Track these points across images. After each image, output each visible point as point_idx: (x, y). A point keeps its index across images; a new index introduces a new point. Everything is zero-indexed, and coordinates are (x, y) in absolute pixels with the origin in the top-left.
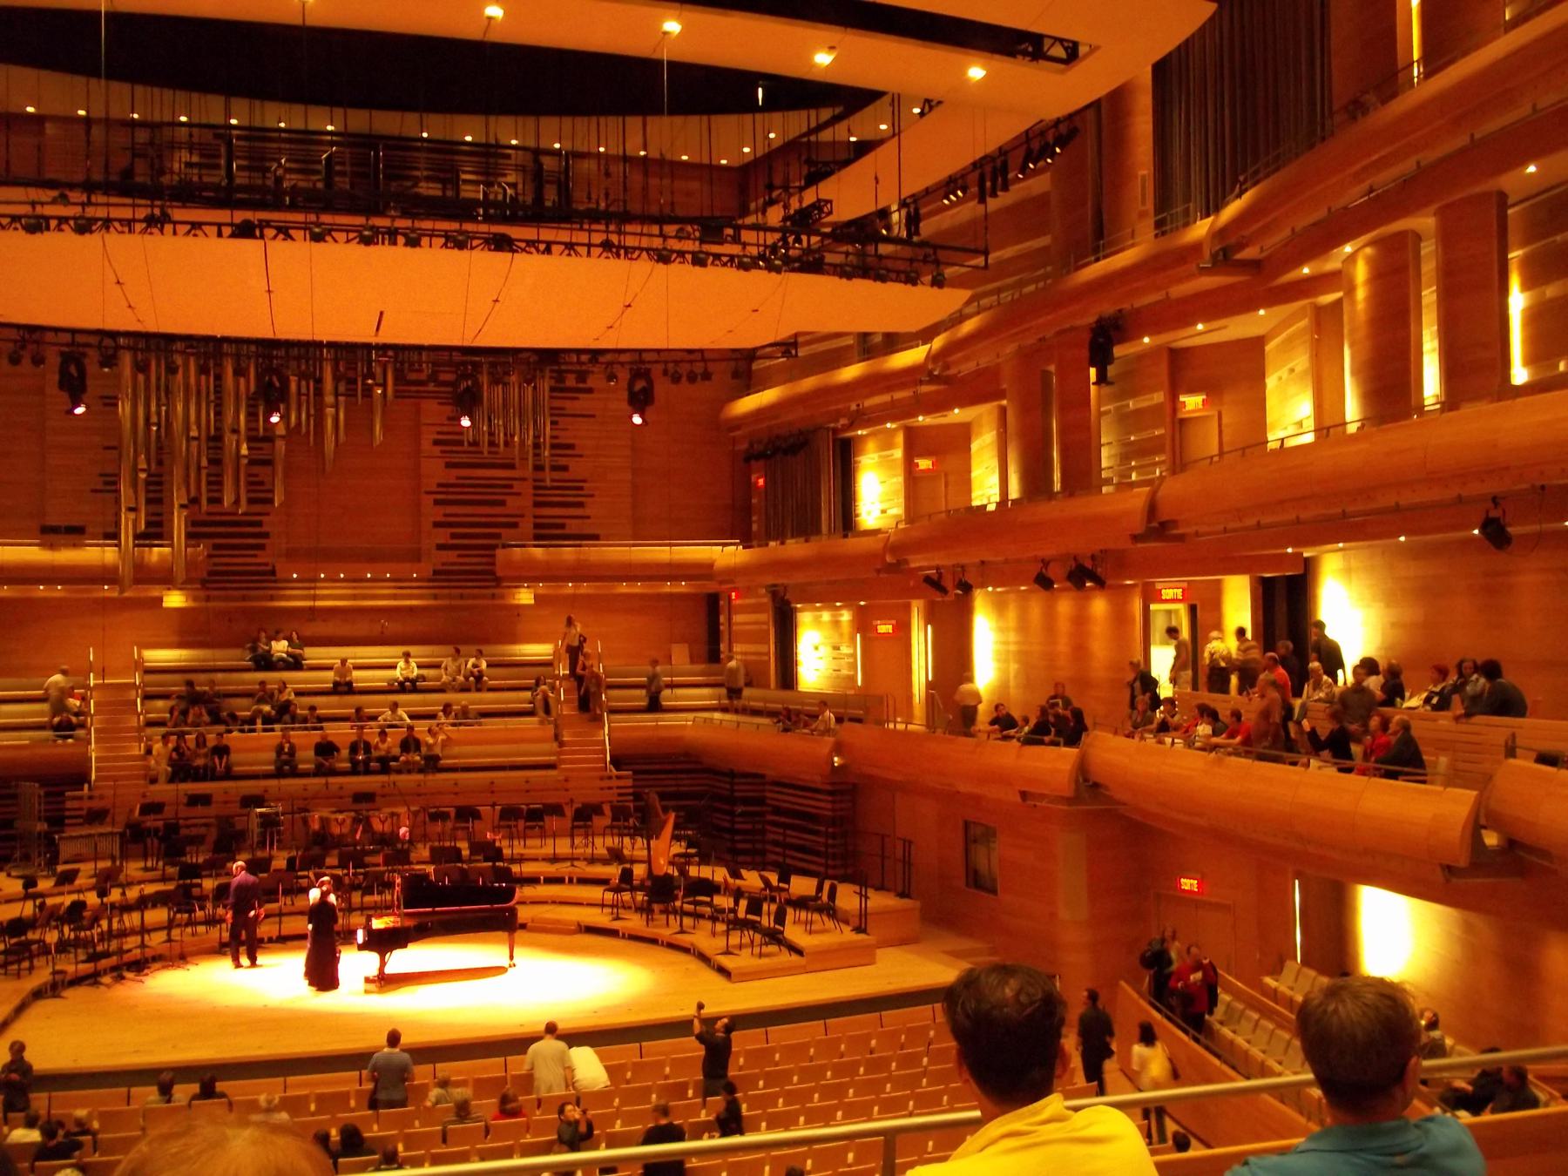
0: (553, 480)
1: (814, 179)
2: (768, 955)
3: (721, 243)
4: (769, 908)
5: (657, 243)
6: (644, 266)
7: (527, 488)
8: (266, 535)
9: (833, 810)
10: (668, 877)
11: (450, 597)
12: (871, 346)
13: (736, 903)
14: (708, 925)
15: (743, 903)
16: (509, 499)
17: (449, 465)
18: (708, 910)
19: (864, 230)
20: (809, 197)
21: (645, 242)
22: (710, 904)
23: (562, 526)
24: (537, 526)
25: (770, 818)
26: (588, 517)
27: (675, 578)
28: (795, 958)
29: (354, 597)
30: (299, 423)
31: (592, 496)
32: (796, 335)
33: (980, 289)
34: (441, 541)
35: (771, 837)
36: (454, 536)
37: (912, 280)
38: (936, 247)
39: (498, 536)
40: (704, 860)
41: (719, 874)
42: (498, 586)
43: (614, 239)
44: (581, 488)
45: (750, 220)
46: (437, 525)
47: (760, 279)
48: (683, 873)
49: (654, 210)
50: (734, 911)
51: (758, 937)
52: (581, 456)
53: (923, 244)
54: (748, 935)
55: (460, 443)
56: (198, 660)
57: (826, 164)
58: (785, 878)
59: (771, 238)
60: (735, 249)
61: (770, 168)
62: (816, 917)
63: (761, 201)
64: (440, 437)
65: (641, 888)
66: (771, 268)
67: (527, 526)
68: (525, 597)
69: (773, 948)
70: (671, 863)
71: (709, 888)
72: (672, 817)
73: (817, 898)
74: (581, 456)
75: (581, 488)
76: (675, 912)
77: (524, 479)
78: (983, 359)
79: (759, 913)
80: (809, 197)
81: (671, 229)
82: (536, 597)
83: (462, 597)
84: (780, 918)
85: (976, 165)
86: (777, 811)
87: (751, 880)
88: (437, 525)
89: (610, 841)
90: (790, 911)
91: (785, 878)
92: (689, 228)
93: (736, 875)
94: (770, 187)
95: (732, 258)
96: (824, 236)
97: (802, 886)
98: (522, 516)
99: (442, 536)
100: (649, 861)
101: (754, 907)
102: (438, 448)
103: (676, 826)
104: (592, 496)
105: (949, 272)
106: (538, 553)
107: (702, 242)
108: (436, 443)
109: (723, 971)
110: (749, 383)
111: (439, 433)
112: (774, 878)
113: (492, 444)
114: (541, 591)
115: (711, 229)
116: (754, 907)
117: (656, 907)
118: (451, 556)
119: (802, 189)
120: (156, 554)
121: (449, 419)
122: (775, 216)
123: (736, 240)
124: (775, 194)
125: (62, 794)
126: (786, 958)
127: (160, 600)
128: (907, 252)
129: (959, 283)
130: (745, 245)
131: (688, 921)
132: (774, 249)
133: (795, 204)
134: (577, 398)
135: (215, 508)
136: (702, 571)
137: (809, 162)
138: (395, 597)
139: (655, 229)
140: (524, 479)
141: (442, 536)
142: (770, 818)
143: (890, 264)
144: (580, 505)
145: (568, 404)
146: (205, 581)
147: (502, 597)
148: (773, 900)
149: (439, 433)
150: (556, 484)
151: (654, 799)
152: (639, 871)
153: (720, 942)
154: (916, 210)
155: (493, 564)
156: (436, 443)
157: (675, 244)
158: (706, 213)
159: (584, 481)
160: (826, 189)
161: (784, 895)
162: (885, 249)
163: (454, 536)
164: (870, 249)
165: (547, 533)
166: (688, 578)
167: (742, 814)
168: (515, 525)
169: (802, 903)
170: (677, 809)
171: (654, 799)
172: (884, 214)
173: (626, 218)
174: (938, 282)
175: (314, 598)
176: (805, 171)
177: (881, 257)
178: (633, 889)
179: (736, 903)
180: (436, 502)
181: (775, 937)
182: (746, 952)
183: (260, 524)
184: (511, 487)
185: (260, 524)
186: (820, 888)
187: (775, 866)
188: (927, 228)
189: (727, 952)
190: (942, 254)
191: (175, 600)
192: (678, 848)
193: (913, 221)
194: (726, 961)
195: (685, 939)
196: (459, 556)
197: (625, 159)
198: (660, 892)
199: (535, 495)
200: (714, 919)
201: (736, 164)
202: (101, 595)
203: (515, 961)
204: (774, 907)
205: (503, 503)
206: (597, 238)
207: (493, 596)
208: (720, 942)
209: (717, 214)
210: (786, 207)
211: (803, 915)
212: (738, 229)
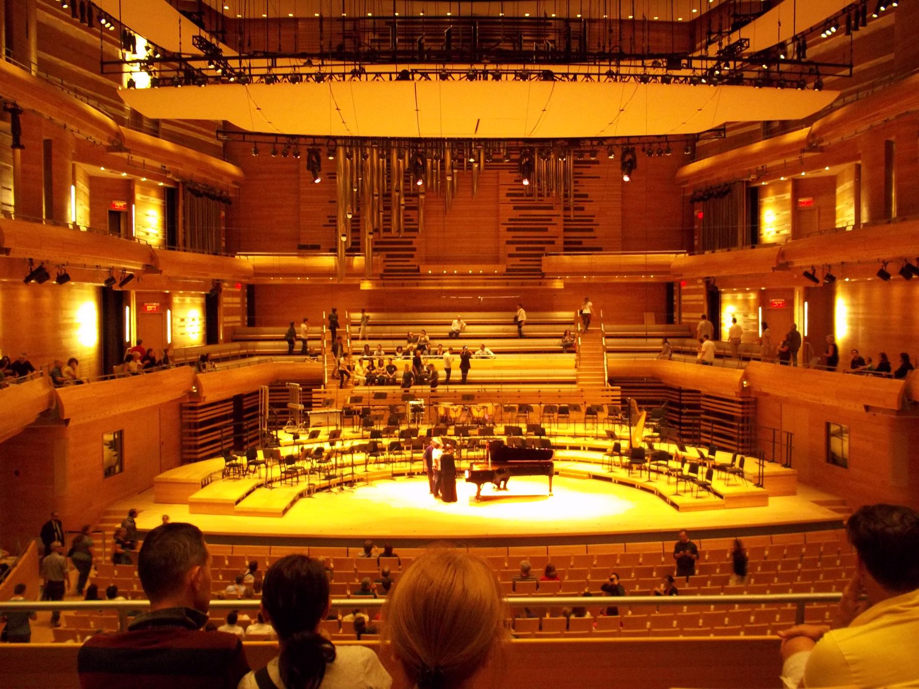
0: (575, 216)
1: (737, 27)
2: (700, 497)
3: (680, 69)
4: (703, 470)
5: (640, 71)
6: (632, 85)
7: (559, 221)
8: (414, 249)
9: (742, 413)
10: (641, 450)
11: (516, 284)
12: (771, 129)
13: (683, 466)
14: (665, 477)
15: (687, 467)
16: (550, 227)
17: (515, 208)
18: (665, 469)
19: (769, 55)
20: (735, 38)
21: (632, 71)
22: (666, 466)
23: (580, 243)
24: (565, 243)
25: (703, 416)
26: (595, 238)
27: (647, 273)
28: (718, 499)
29: (463, 284)
30: (432, 186)
32: (725, 124)
33: (845, 91)
35: (702, 428)
36: (518, 249)
37: (802, 85)
38: (817, 65)
39: (543, 249)
40: (663, 439)
41: (672, 448)
42: (543, 278)
43: (614, 69)
44: (592, 221)
45: (696, 54)
46: (508, 243)
47: (705, 91)
48: (651, 447)
49: (638, 51)
50: (681, 470)
51: (695, 486)
52: (592, 201)
53: (810, 63)
54: (689, 485)
55: (522, 195)
57: (746, 16)
58: (712, 452)
59: (710, 64)
60: (688, 72)
61: (710, 21)
62: (731, 476)
63: (704, 41)
64: (509, 192)
65: (626, 454)
66: (709, 83)
67: (560, 242)
68: (559, 284)
69: (704, 493)
70: (644, 441)
71: (666, 456)
72: (645, 413)
73: (732, 465)
74: (592, 201)
76: (646, 469)
77: (559, 216)
78: (847, 133)
79: (696, 472)
80: (735, 38)
81: (649, 62)
82: (567, 286)
83: (522, 284)
84: (709, 476)
85: (844, 10)
86: (708, 413)
87: (692, 452)
88: (508, 243)
89: (609, 427)
90: (715, 472)
91: (712, 452)
92: (660, 61)
93: (682, 449)
94: (710, 33)
95: (686, 77)
96: (745, 61)
97: (722, 457)
99: (512, 249)
100: (630, 440)
101: (694, 469)
102: (509, 198)
103: (647, 420)
105: (825, 80)
106: (567, 259)
107: (668, 68)
109: (673, 505)
110: (833, 82)
111: (509, 189)
112: (705, 452)
114: (569, 281)
115: (674, 63)
116: (694, 469)
117: (634, 466)
118: (516, 261)
119: (729, 33)
120: (358, 261)
121: (516, 181)
122: (713, 50)
123: (689, 66)
124: (712, 37)
125: (310, 390)
126: (712, 498)
127: (359, 286)
128: (798, 68)
129: (832, 87)
130: (694, 69)
131: (653, 475)
132: (712, 70)
133: (725, 43)
134: (590, 167)
136: (664, 269)
137: (735, 16)
138: (485, 284)
139: (639, 63)
140: (559, 216)
141: (512, 249)
142: (703, 416)
143: (786, 77)
144: (591, 230)
145: (583, 170)
147: (545, 284)
148: (705, 465)
149: (509, 189)
151: (634, 402)
152: (624, 445)
153: (673, 489)
154: (804, 42)
155: (540, 265)
156: (508, 195)
157: (651, 71)
158: (670, 52)
159: (594, 216)
160: (745, 32)
161: (712, 463)
162: (784, 67)
163: (518, 249)
164: (774, 68)
165: (572, 247)
167: (687, 414)
168: (553, 243)
169: (722, 468)
170: (647, 409)
171: (634, 402)
172: (782, 46)
173: (619, 57)
174: (819, 86)
176: (732, 20)
177: (781, 73)
178: (621, 455)
179: (683, 466)
180: (509, 230)
181: (705, 486)
182: (689, 495)
183: (411, 243)
184: (551, 220)
185: (411, 243)
186: (734, 459)
187: (707, 445)
188: (811, 53)
189: (677, 494)
190: (821, 69)
191: (366, 286)
192: (648, 432)
193: (801, 49)
194: (676, 500)
195: (651, 485)
196: (521, 261)
197: (621, 22)
198: (637, 456)
199: (565, 225)
200: (668, 474)
201: (688, 20)
203: (552, 492)
204: (705, 469)
205: (546, 230)
206: (604, 70)
207: (540, 284)
208: (673, 489)
209: (676, 51)
210: (720, 44)
211: (723, 475)
212: (690, 60)
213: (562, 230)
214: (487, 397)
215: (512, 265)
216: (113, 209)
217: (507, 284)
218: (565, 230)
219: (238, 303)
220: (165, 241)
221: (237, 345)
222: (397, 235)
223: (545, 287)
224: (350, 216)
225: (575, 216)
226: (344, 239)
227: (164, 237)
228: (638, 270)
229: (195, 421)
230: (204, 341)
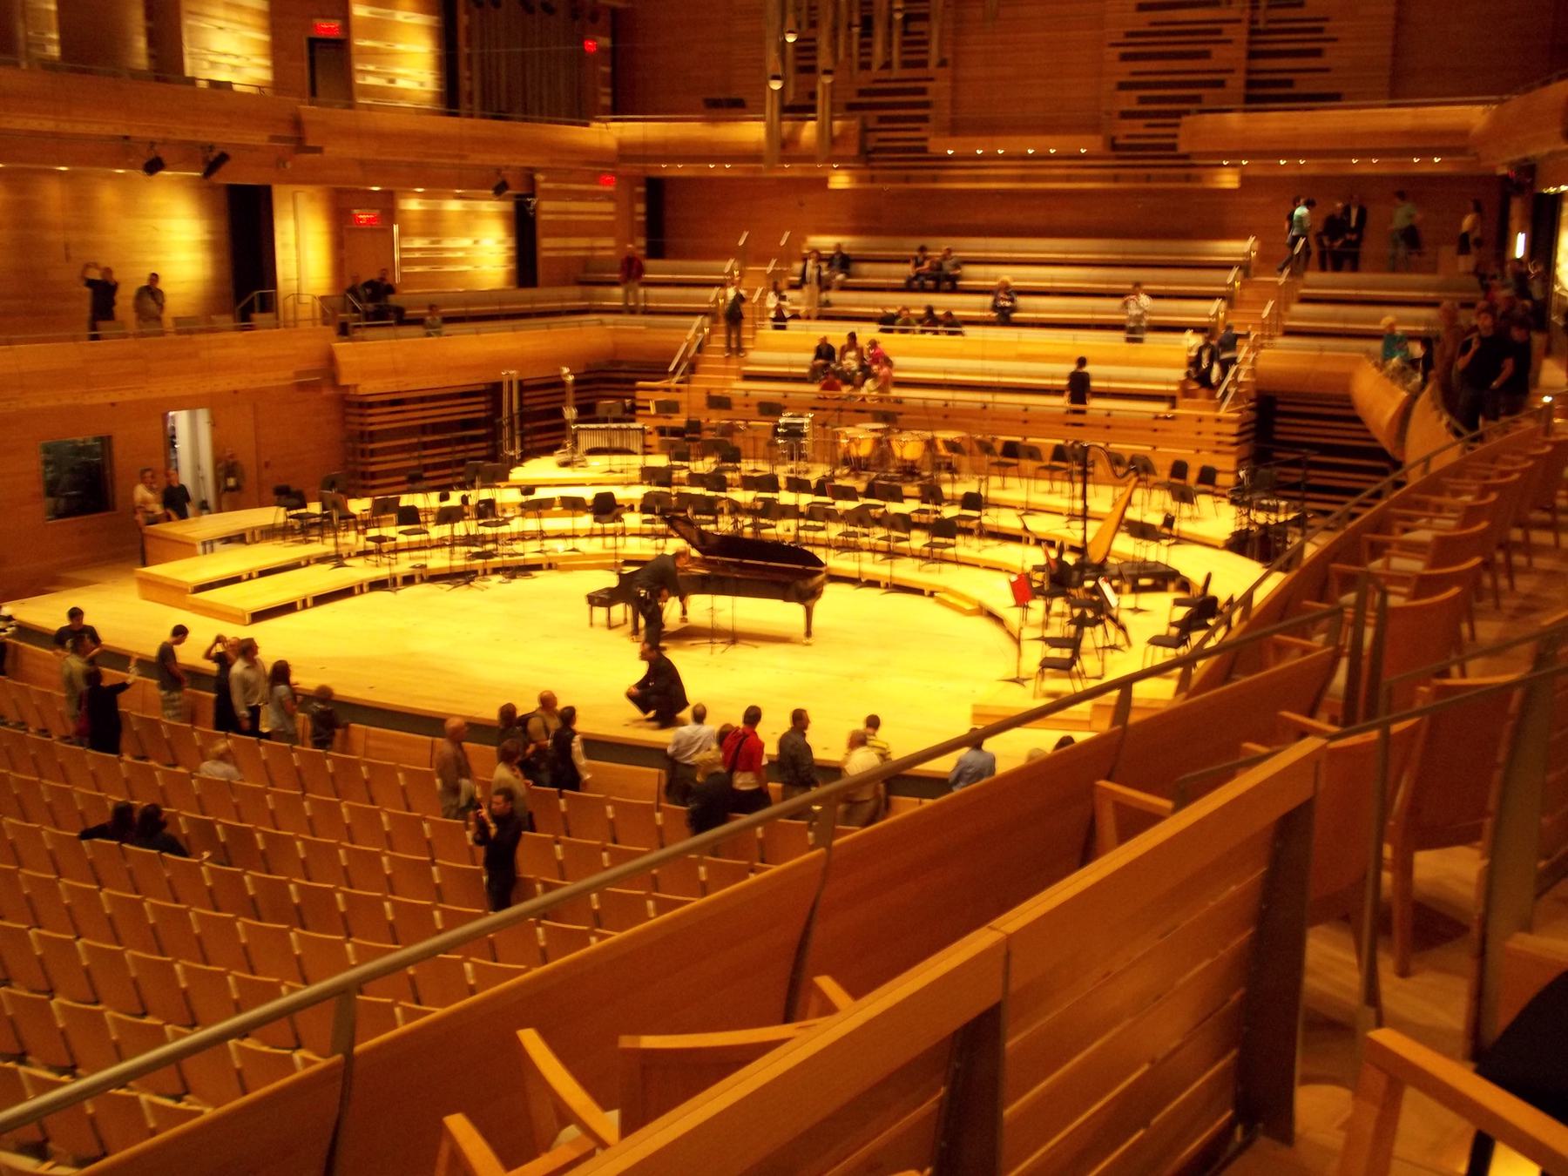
0: (1270, 21)
7: (1239, 34)
8: (926, 105)
11: (1137, 179)
23: (1289, 83)
24: (1250, 84)
26: (1326, 70)
27: (1427, 153)
29: (1022, 179)
31: (1335, 40)
34: (1126, 108)
36: (1143, 100)
39: (1196, 99)
44: (1320, 30)
46: (1123, 86)
56: (859, 249)
67: (1236, 82)
68: (1228, 180)
75: (1320, 30)
77: (1238, 21)
82: (1245, 180)
83: (1148, 178)
88: (1123, 86)
98: (1231, 71)
99: (1129, 100)
104: (1335, 40)
106: (1234, 120)
114: (1253, 172)
118: (1138, 126)
127: (825, 181)
135: (885, 74)
136: (1453, 142)
138: (1068, 179)
140: (1238, 21)
141: (1129, 100)
144: (1317, 53)
146: (866, 157)
147: (1199, 179)
150: (1272, 26)
159: (1326, 19)
163: (1143, 100)
165: (1260, 95)
166: (1307, 154)
168: (1220, 84)
175: (978, 179)
180: (1125, 57)
183: (923, 91)
184: (1219, 32)
185: (923, 91)
191: (840, 180)
196: (1149, 126)
202: (780, 174)
205: (1206, 55)
207: (1188, 178)
213: (1243, 54)
214: (947, 417)
215: (1128, 137)
216: (314, 35)
217: (1116, 179)
218: (1252, 55)
219: (610, 213)
220: (440, 94)
221: (576, 291)
222: (885, 74)
223: (1198, 186)
224: (791, 39)
225: (1270, 21)
226: (776, 85)
227: (441, 87)
228: (1387, 144)
229: (363, 428)
230: (509, 283)
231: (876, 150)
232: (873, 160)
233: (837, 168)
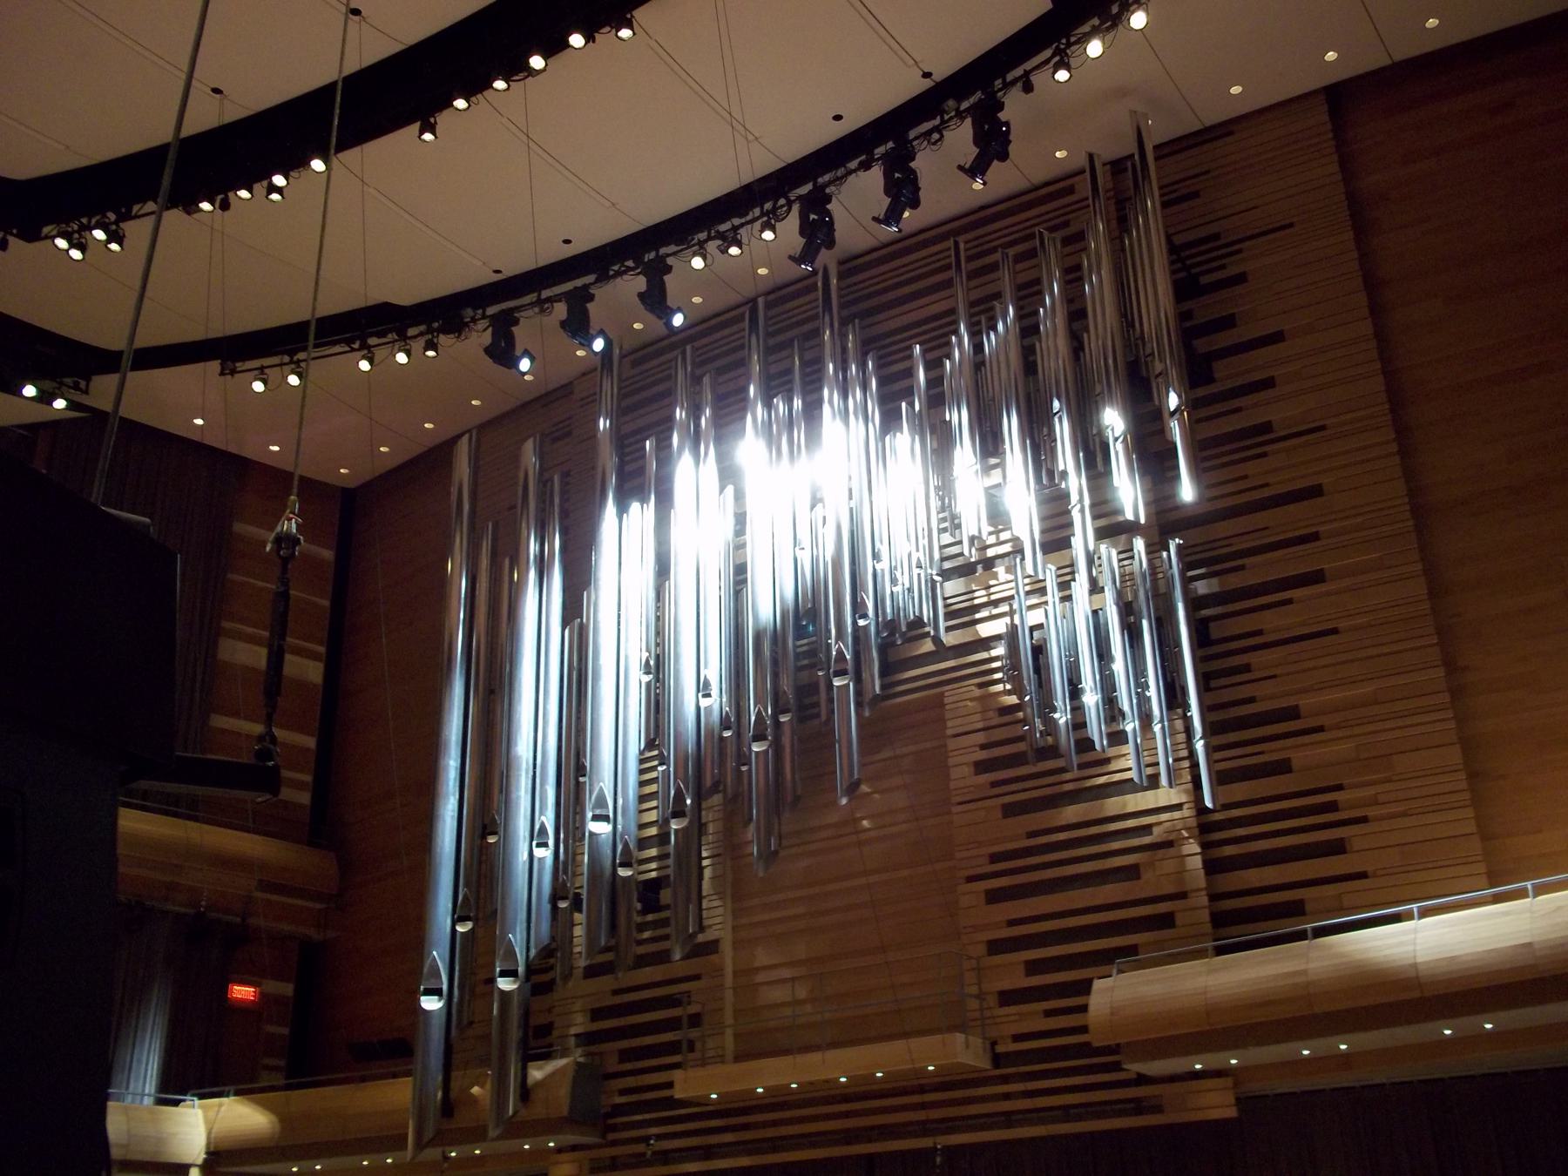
17: (1010, 811)
34: (1006, 985)
36: (1033, 968)
44: (1332, 807)
46: (996, 947)
75: (1332, 807)
88: (996, 947)
98: (1183, 895)
99: (1011, 972)
108: (981, 767)
113: (1085, 745)
114: (1256, 1087)
118: (1031, 1017)
141: (1011, 972)
144: (1338, 848)
159: (1339, 788)
163: (1033, 968)
168: (1167, 921)
180: (994, 897)
196: (1049, 1013)
207: (1138, 1107)
215: (1017, 1038)
231: (618, 1110)
232: (614, 1128)
233: (559, 1150)
